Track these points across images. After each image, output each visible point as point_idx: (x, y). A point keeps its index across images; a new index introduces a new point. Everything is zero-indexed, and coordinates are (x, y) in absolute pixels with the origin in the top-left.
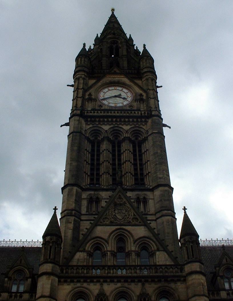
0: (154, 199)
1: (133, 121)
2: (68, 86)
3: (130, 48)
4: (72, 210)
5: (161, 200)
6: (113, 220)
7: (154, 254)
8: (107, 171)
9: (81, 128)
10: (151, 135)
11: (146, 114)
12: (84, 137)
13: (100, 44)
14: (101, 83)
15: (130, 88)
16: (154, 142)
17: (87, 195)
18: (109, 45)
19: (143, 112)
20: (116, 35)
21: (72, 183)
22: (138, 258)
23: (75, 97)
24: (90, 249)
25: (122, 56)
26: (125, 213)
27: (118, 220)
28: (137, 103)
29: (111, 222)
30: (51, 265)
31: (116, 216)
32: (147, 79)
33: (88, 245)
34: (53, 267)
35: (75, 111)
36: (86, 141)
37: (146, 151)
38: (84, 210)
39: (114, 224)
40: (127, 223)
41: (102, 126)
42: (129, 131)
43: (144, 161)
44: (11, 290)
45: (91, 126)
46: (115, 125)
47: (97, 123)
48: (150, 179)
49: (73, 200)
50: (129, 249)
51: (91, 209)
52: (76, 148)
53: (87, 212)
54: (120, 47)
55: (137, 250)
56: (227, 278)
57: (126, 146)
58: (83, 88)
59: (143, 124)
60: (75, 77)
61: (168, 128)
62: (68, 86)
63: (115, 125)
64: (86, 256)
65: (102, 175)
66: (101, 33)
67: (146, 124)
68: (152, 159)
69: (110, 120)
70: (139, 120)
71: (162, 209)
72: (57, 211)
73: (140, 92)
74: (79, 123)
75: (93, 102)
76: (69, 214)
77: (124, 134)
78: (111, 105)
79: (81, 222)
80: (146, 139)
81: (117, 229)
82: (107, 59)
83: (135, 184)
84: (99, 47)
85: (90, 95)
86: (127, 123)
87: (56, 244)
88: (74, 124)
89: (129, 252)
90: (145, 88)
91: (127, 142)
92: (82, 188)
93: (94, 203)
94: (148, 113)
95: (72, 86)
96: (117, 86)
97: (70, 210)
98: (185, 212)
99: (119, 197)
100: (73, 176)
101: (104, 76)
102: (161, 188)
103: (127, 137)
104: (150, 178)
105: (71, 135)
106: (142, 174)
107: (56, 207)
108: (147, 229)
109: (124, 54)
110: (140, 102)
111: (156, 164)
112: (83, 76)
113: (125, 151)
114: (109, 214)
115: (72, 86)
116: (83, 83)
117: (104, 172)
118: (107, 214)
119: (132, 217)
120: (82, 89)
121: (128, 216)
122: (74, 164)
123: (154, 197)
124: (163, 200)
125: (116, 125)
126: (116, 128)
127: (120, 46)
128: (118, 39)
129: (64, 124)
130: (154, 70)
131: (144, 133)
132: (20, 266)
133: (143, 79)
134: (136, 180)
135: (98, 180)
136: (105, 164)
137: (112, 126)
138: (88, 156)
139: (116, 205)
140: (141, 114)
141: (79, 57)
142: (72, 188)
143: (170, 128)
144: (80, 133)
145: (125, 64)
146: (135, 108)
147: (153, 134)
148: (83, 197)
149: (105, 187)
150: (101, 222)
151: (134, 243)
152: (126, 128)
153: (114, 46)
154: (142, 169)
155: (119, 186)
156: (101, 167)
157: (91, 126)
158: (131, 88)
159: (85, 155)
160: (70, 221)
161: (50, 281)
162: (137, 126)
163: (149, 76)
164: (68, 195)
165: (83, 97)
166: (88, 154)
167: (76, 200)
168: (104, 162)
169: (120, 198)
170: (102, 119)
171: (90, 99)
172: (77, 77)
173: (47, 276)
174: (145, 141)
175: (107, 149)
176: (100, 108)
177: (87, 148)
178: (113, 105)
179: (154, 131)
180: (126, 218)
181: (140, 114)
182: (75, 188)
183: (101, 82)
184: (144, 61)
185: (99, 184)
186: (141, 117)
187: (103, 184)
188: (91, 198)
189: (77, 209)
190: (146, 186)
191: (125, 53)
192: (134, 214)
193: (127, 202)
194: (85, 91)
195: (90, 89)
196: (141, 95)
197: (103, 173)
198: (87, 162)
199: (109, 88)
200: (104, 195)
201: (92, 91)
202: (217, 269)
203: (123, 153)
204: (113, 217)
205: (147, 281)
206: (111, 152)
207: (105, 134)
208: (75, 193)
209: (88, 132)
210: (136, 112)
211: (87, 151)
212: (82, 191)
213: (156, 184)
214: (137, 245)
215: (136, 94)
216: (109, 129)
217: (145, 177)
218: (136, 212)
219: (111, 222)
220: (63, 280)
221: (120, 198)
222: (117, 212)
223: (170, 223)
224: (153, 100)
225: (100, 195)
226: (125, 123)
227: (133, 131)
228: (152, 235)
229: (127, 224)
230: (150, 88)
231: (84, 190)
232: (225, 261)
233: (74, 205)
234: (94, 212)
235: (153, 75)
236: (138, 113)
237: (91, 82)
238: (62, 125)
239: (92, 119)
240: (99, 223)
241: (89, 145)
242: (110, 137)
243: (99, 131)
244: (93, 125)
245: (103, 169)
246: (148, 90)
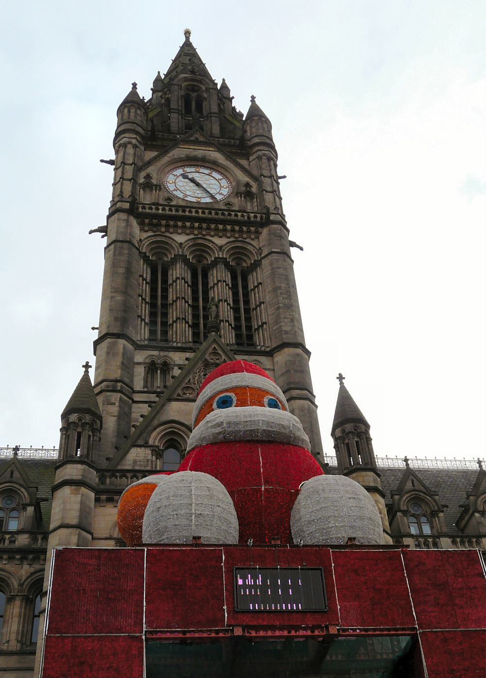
0: (274, 369)
1: (233, 230)
2: (102, 161)
3: (224, 103)
4: (117, 381)
5: (288, 371)
8: (184, 317)
10: (268, 257)
11: (259, 219)
12: (138, 252)
13: (165, 90)
14: (169, 157)
15: (227, 171)
16: (273, 269)
17: (145, 356)
18: (182, 93)
19: (252, 215)
20: (197, 74)
21: (115, 331)
23: (118, 179)
24: (159, 442)
25: (209, 115)
28: (239, 198)
32: (259, 158)
33: (155, 433)
35: (118, 204)
36: (142, 260)
37: (257, 286)
38: (138, 384)
41: (172, 236)
42: (226, 248)
43: (254, 304)
45: (150, 234)
46: (197, 235)
47: (163, 229)
48: (266, 335)
51: (152, 382)
52: (122, 270)
54: (205, 98)
56: (413, 515)
57: (219, 275)
58: (134, 163)
59: (253, 236)
60: (116, 142)
61: (299, 249)
62: (102, 161)
63: (197, 235)
64: (150, 457)
65: (172, 325)
66: (165, 74)
67: (258, 239)
68: (270, 298)
69: (188, 224)
70: (245, 229)
71: (292, 386)
73: (244, 178)
75: (154, 191)
76: (111, 389)
77: (216, 251)
78: (189, 199)
79: (134, 405)
80: (257, 264)
82: (180, 117)
83: (237, 344)
84: (163, 96)
85: (148, 177)
86: (221, 234)
87: (90, 428)
88: (118, 227)
90: (255, 172)
91: (221, 267)
92: (133, 343)
93: (159, 371)
94: (261, 218)
95: (111, 162)
96: (201, 166)
98: (341, 384)
99: (213, 351)
100: (116, 319)
101: (175, 144)
102: (287, 351)
103: (220, 258)
104: (265, 333)
105: (113, 246)
106: (249, 328)
109: (212, 111)
110: (245, 198)
112: (134, 141)
113: (217, 284)
115: (111, 162)
116: (135, 154)
117: (177, 318)
118: (190, 379)
120: (131, 165)
122: (119, 298)
123: (274, 367)
124: (292, 371)
125: (200, 236)
126: (200, 241)
127: (205, 95)
128: (200, 82)
129: (97, 228)
130: (272, 141)
131: (254, 253)
133: (250, 158)
134: (238, 336)
135: (165, 333)
136: (178, 304)
137: (192, 236)
138: (144, 288)
139: (207, 364)
140: (249, 218)
141: (126, 107)
142: (115, 343)
143: (301, 249)
144: (130, 242)
145: (216, 130)
146: (236, 208)
147: (273, 254)
148: (136, 361)
149: (179, 345)
150: (179, 395)
152: (220, 241)
153: (194, 95)
154: (248, 319)
155: (213, 331)
156: (171, 311)
157: (150, 234)
158: (230, 173)
159: (140, 285)
160: (113, 401)
162: (241, 239)
163: (263, 152)
164: (108, 353)
165: (134, 180)
166: (144, 285)
167: (123, 363)
168: (176, 301)
170: (172, 223)
171: (148, 186)
172: (122, 142)
173: (73, 488)
174: (256, 268)
175: (183, 276)
176: (169, 203)
177: (143, 273)
178: (194, 200)
181: (246, 218)
182: (122, 342)
183: (170, 154)
184: (253, 125)
185: (167, 341)
186: (249, 223)
187: (175, 340)
188: (153, 363)
189: (126, 380)
190: (259, 348)
191: (215, 109)
194: (138, 169)
195: (148, 167)
196: (247, 185)
197: (175, 319)
198: (143, 299)
199: (186, 169)
200: (178, 358)
201: (152, 170)
202: (397, 497)
203: (213, 287)
206: (190, 283)
207: (178, 249)
208: (121, 350)
209: (144, 244)
210: (239, 214)
211: (143, 279)
212: (135, 349)
213: (279, 343)
215: (238, 182)
216: (186, 241)
217: (255, 331)
220: (105, 497)
221: (215, 353)
223: (306, 412)
224: (271, 194)
225: (170, 358)
226: (218, 233)
227: (233, 248)
230: (265, 173)
231: (139, 347)
232: (411, 485)
233: (119, 371)
234: (158, 387)
235: (270, 150)
236: (243, 216)
237: (150, 155)
238: (92, 229)
239: (154, 221)
241: (147, 269)
242: (188, 257)
243: (167, 243)
244: (154, 232)
245: (175, 312)
246: (261, 176)
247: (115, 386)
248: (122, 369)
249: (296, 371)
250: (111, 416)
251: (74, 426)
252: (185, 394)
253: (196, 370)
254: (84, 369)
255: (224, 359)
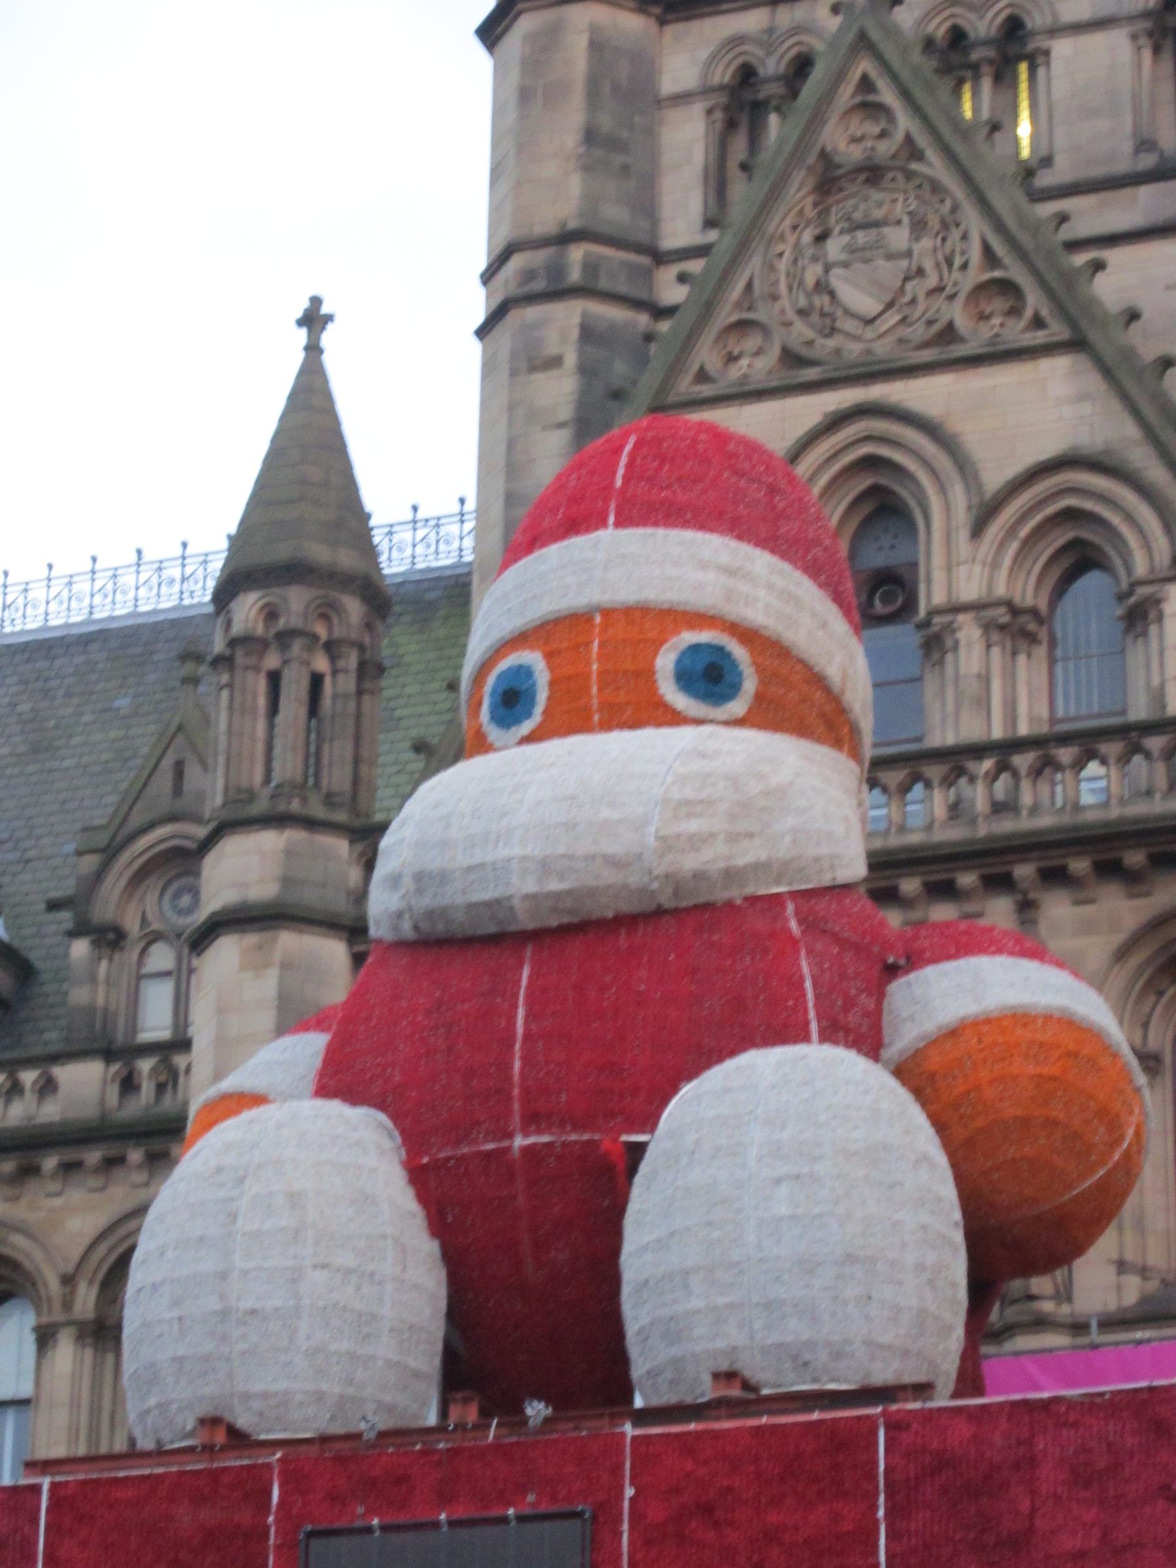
4: (566, 238)
6: (810, 334)
7: (1152, 615)
22: (1022, 659)
26: (909, 254)
27: (849, 325)
29: (792, 359)
30: (270, 840)
31: (832, 294)
34: (289, 853)
39: (810, 374)
40: (926, 345)
44: (133, 1030)
49: (571, 140)
50: (939, 598)
53: (710, 223)
55: (1001, 590)
72: (327, 339)
81: (836, 421)
89: (937, 620)
99: (858, 99)
107: (316, 301)
108: (1094, 381)
114: (776, 283)
119: (976, 275)
121: (932, 281)
132: (173, 818)
150: (702, 376)
151: (978, 530)
160: (552, 347)
161: (272, 977)
167: (591, 136)
169: (864, 105)
180: (913, 301)
188: (747, 74)
189: (615, 215)
192: (988, 252)
193: (922, 140)
204: (802, 302)
205: (1055, 876)
214: (1002, 546)
218: (1000, 226)
219: (792, 359)
222: (843, 257)
228: (1130, 430)
229: (927, 355)
233: (575, 185)
240: (685, 386)
247: (557, 270)
248: (587, 169)
250: (545, 428)
251: (248, 654)
252: (732, 359)
253: (780, 221)
254: (303, 333)
255: (909, 140)
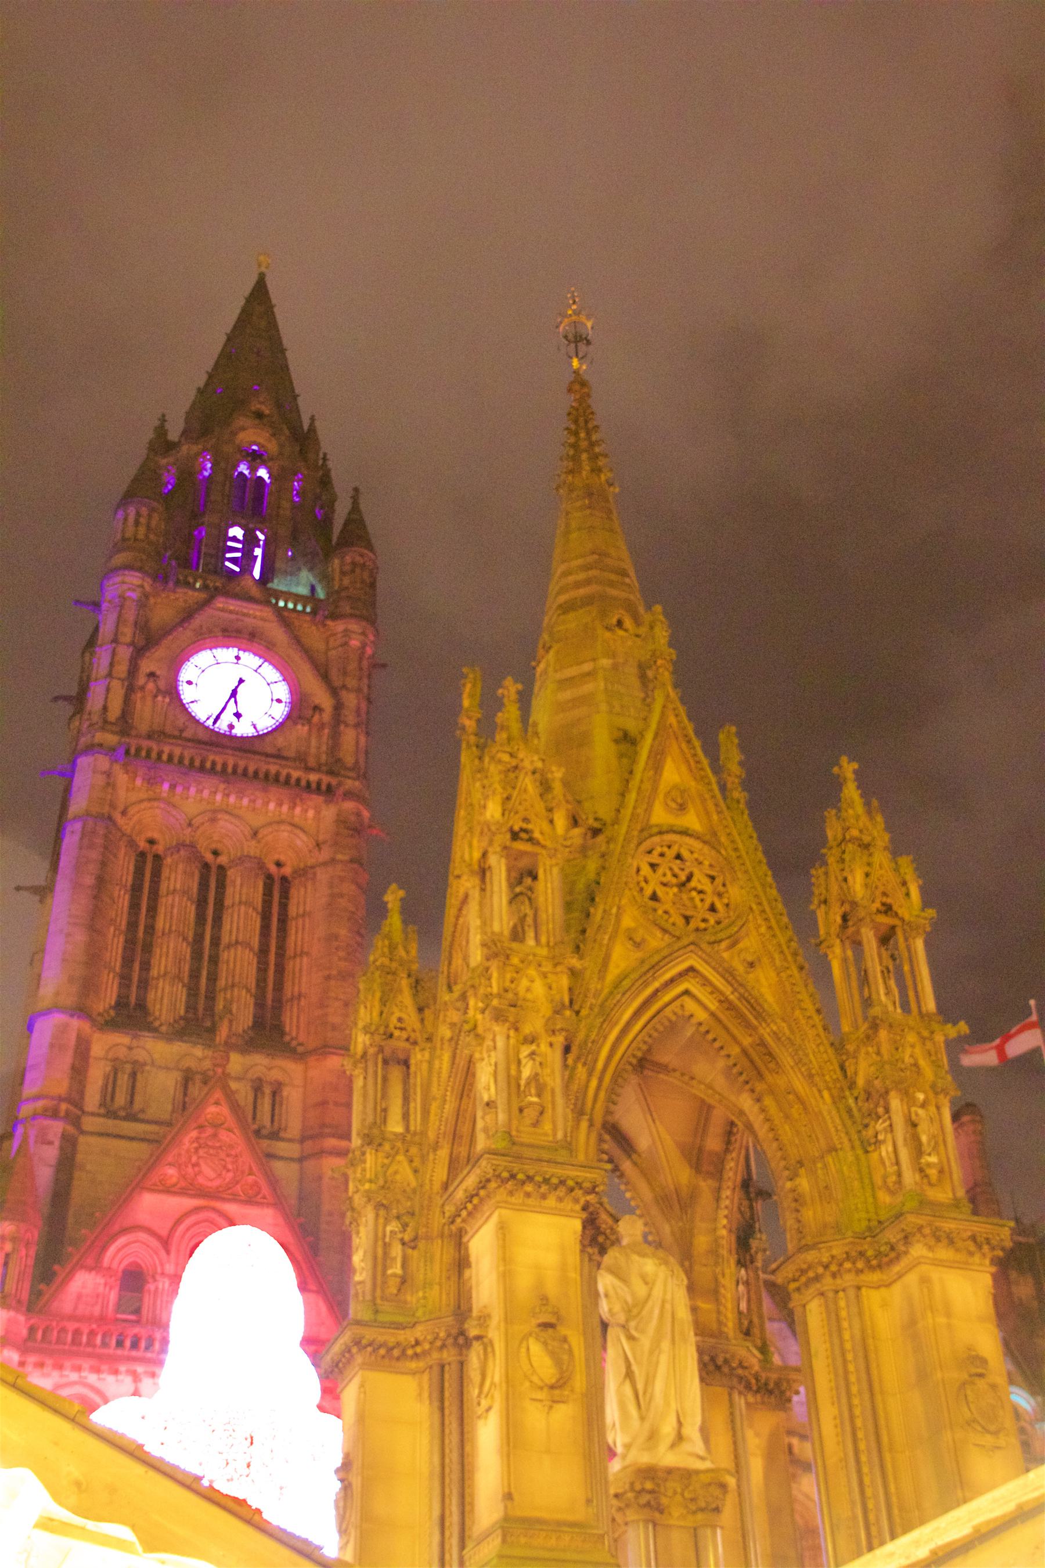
4: (61, 1099)
5: (324, 1103)
9: (113, 806)
16: (333, 896)
52: (89, 880)
74: (108, 784)
79: (82, 1139)
81: (197, 1210)
97: (52, 1098)
100: (71, 980)
111: (328, 978)
136: (172, 945)
179: (339, 857)
230: (352, 683)
249: (336, 1104)
